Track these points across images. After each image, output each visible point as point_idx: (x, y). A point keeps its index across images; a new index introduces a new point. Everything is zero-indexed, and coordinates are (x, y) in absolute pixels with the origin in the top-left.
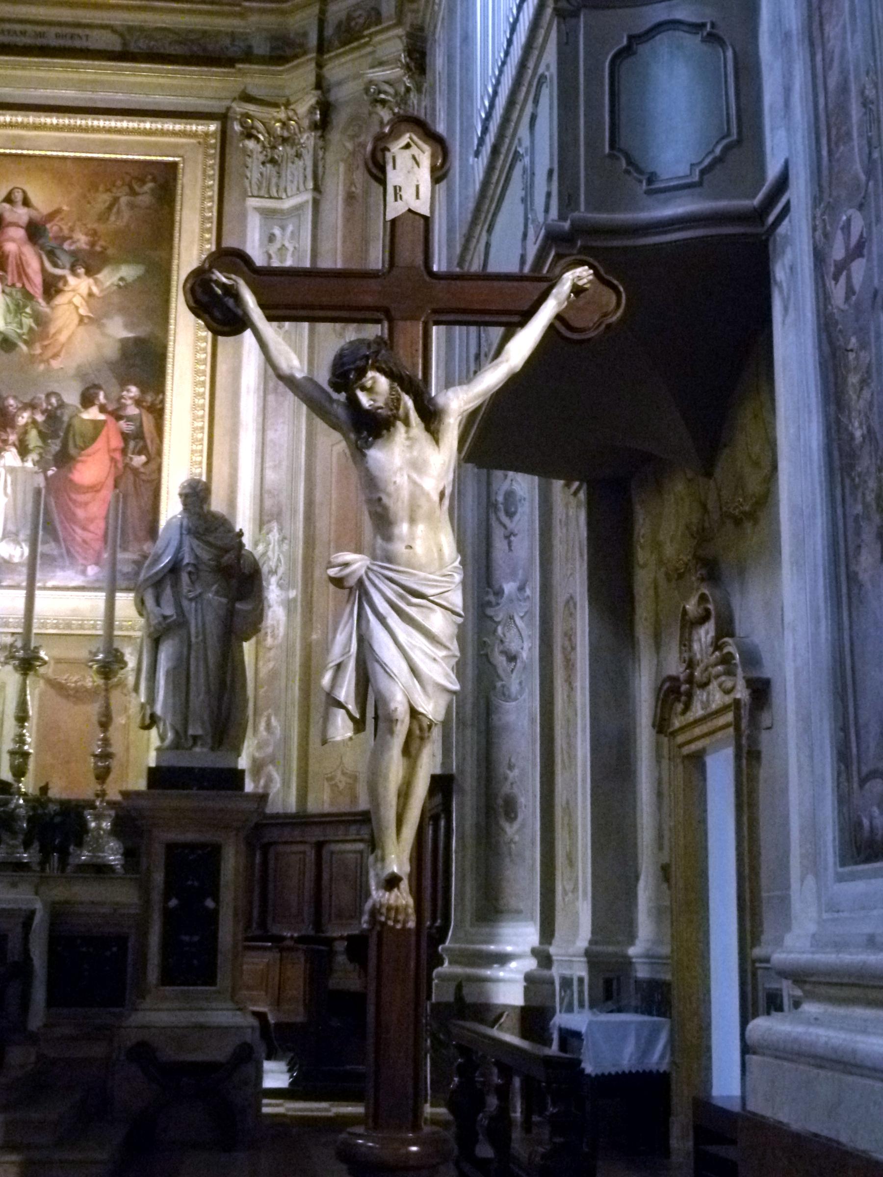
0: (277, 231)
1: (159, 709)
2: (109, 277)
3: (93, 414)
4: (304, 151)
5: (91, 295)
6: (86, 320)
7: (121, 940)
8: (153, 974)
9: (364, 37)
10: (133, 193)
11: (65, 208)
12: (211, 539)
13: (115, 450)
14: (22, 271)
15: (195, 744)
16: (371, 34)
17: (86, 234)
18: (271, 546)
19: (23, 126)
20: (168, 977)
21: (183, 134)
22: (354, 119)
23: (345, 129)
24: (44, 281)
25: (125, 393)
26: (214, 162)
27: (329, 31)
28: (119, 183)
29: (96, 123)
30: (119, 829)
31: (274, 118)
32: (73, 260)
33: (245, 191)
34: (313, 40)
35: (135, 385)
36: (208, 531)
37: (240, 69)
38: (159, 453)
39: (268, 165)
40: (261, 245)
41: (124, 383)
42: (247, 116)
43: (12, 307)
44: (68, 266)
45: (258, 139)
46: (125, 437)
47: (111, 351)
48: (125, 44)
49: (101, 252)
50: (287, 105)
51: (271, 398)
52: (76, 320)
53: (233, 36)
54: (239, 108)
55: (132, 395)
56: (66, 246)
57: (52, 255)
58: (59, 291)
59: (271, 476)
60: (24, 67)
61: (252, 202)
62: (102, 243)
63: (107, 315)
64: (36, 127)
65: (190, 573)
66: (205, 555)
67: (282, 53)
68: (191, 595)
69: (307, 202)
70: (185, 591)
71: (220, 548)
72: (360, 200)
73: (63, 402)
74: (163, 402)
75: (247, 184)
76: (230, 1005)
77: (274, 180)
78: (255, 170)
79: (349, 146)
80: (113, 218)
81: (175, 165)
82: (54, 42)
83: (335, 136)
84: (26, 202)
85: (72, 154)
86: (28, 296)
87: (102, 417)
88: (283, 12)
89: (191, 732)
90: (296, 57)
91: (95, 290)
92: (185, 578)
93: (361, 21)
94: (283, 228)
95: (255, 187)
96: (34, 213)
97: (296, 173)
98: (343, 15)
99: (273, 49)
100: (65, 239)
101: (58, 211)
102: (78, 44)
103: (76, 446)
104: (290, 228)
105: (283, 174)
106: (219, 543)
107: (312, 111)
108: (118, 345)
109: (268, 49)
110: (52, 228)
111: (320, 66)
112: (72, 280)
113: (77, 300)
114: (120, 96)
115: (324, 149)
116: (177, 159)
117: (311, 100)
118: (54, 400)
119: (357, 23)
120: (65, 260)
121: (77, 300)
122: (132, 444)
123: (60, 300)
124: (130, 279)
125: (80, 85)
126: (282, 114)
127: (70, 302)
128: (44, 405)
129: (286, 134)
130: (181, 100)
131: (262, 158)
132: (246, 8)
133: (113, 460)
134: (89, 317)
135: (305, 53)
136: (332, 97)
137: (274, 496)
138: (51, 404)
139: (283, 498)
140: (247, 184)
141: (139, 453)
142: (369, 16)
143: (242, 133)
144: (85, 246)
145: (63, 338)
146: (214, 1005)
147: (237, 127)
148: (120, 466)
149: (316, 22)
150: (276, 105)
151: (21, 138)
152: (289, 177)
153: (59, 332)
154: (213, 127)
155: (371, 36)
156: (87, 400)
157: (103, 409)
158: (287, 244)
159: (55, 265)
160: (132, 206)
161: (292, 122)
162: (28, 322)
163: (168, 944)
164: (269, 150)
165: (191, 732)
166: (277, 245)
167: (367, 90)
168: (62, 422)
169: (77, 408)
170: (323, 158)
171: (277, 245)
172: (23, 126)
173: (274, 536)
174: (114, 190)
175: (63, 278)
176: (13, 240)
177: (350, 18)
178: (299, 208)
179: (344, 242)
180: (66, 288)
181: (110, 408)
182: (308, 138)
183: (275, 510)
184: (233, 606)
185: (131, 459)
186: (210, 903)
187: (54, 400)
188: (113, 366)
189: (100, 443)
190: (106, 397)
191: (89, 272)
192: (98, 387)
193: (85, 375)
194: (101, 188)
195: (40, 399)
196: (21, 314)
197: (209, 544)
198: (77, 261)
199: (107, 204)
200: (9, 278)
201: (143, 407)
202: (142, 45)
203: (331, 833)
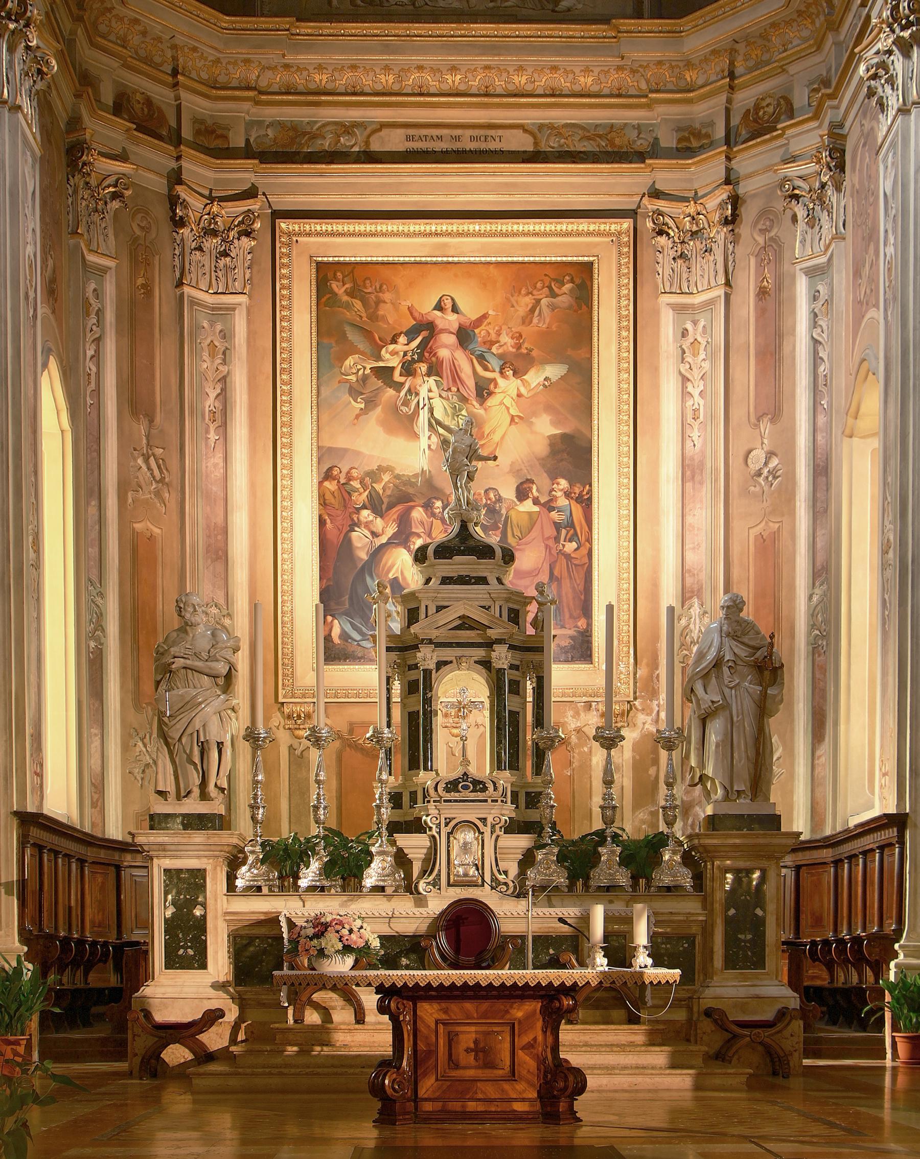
0: (689, 326)
1: (709, 771)
2: (535, 378)
3: (528, 506)
4: (714, 246)
5: (519, 395)
6: (517, 420)
7: (691, 939)
8: (718, 961)
9: (777, 130)
10: (553, 295)
11: (491, 312)
12: (746, 640)
13: (549, 538)
14: (456, 377)
15: (739, 796)
16: (784, 127)
17: (512, 338)
18: (692, 620)
19: (449, 234)
20: (731, 962)
21: (599, 234)
22: (765, 213)
23: (756, 223)
24: (476, 384)
25: (555, 486)
26: (626, 260)
27: (735, 121)
28: (539, 285)
29: (515, 227)
30: (687, 859)
31: (683, 212)
32: (501, 363)
33: (657, 287)
34: (720, 132)
35: (564, 477)
36: (744, 634)
37: (650, 165)
38: (589, 540)
39: (680, 261)
40: (675, 341)
41: (553, 478)
42: (661, 214)
43: (449, 411)
44: (498, 369)
45: (668, 234)
46: (557, 526)
47: (542, 448)
48: (536, 144)
49: (528, 354)
50: (696, 198)
51: (689, 485)
52: (509, 419)
53: (639, 128)
54: (650, 205)
55: (561, 487)
56: (494, 350)
57: (481, 358)
58: (490, 394)
59: (689, 556)
60: (443, 174)
61: (665, 299)
62: (526, 345)
63: (535, 414)
64: (460, 234)
65: (730, 667)
66: (742, 652)
67: (688, 145)
68: (732, 684)
69: (720, 296)
70: (726, 682)
71: (753, 648)
72: (773, 295)
73: (500, 496)
74: (590, 492)
75: (660, 281)
76: (777, 983)
77: (685, 276)
78: (666, 265)
79: (760, 240)
80: (535, 320)
81: (591, 264)
82: (472, 146)
83: (744, 230)
84: (455, 309)
85: (494, 259)
86: (464, 399)
87: (536, 509)
88: (689, 101)
89: (736, 788)
90: (702, 148)
91: (523, 391)
92: (725, 669)
93: (770, 110)
94: (695, 323)
95: (667, 284)
96: (463, 320)
97: (706, 267)
98: (750, 104)
99: (680, 140)
100: (492, 343)
101: (485, 316)
102: (493, 146)
103: (513, 535)
104: (702, 323)
105: (693, 269)
106: (752, 643)
107: (722, 206)
108: (547, 442)
109: (675, 142)
110: (480, 333)
111: (729, 159)
112: (500, 381)
113: (508, 401)
114: (535, 198)
115: (735, 242)
116: (591, 259)
118: (492, 495)
119: (765, 112)
120: (495, 363)
121: (508, 401)
122: (564, 532)
123: (492, 402)
124: (554, 379)
126: (692, 209)
127: (502, 403)
128: (484, 501)
129: (695, 228)
130: (592, 198)
131: (672, 253)
132: (651, 99)
133: (547, 547)
134: (518, 416)
135: (712, 145)
136: (741, 191)
137: (694, 575)
138: (490, 499)
139: (704, 577)
140: (660, 281)
141: (570, 541)
142: (779, 104)
143: (654, 230)
144: (511, 349)
145: (496, 437)
146: (765, 982)
147: (649, 225)
148: (554, 552)
149: (723, 112)
150: (685, 200)
151: (445, 245)
152: (699, 272)
153: (493, 431)
154: (626, 224)
155: (784, 129)
156: (522, 494)
157: (536, 502)
158: (699, 339)
159: (486, 369)
160: (553, 307)
161: (701, 216)
163: (730, 941)
164: (679, 245)
165: (736, 788)
166: (690, 339)
167: (782, 186)
168: (502, 515)
169: (513, 501)
170: (733, 252)
171: (690, 339)
172: (449, 234)
173: (696, 610)
174: (535, 292)
175: (494, 380)
176: (446, 346)
177: (757, 107)
178: (711, 302)
179: (756, 336)
180: (497, 390)
181: (543, 500)
182: (718, 232)
183: (696, 587)
184: (766, 692)
185: (564, 546)
186: (759, 912)
187: (492, 495)
188: (542, 461)
189: (535, 533)
190: (538, 490)
191: (516, 373)
192: (532, 482)
193: (518, 471)
194: (523, 291)
195: (480, 494)
196: (458, 416)
197: (743, 643)
198: (505, 363)
199: (530, 306)
200: (445, 382)
201: (572, 498)
202: (552, 144)
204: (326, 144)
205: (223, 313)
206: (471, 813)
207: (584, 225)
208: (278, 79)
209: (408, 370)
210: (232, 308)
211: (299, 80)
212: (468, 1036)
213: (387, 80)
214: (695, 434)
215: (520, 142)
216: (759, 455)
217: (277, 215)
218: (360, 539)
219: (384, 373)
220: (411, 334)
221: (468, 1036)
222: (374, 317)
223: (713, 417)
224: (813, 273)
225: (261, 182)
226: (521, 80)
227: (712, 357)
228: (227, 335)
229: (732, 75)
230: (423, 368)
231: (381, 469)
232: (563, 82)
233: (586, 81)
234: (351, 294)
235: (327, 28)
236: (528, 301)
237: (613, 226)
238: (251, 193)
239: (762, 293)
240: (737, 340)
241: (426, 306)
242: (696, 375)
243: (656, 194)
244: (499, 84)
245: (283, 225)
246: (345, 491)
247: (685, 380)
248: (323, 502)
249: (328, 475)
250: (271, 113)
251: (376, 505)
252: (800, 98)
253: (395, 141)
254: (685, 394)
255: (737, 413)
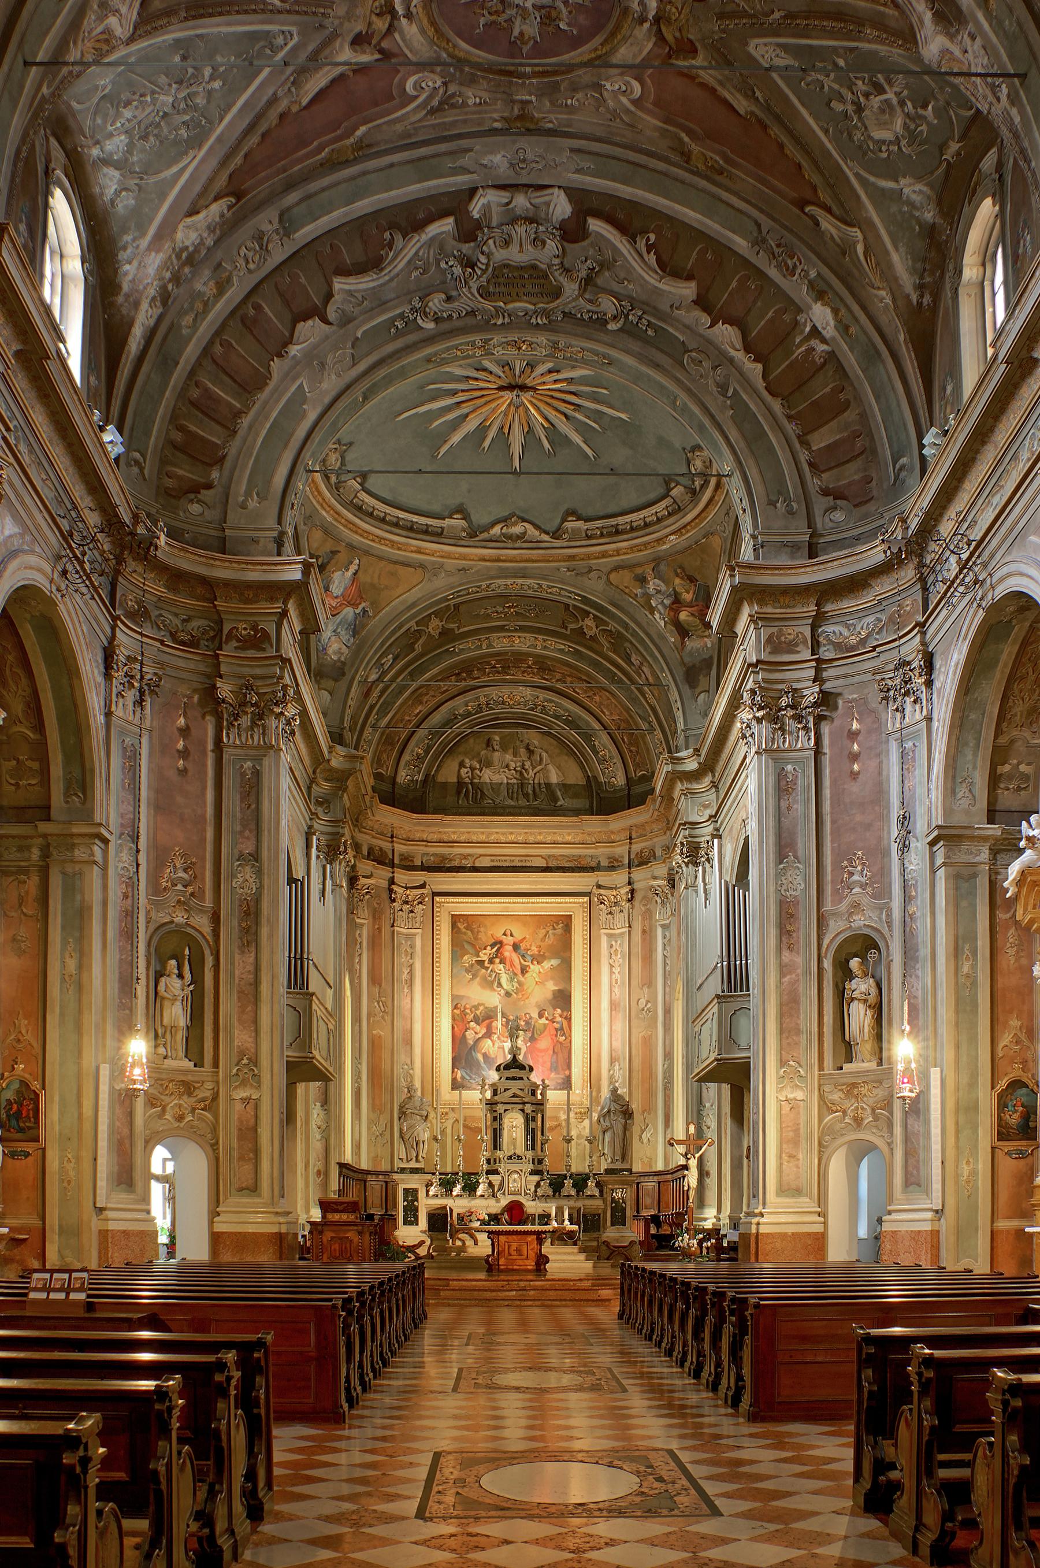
2: (547, 965)
3: (543, 1021)
14: (512, 964)
22: (644, 898)
34: (626, 861)
47: (550, 996)
54: (596, 891)
57: (523, 956)
78: (603, 917)
83: (636, 903)
110: (523, 946)
117: (627, 889)
120: (529, 959)
125: (530, 883)
154: (586, 899)
156: (541, 1016)
162: (516, 985)
178: (622, 934)
188: (550, 1001)
203: (642, 1179)
204: (456, 863)
205: (411, 937)
206: (517, 1168)
207: (568, 899)
208: (435, 837)
209: (491, 961)
210: (415, 935)
211: (445, 838)
212: (514, 1246)
213: (483, 838)
214: (616, 990)
215: (541, 863)
216: (643, 1001)
217: (435, 894)
218: (470, 1034)
219: (481, 963)
220: (493, 946)
221: (514, 1246)
222: (476, 939)
223: (623, 983)
224: (664, 927)
225: (428, 881)
226: (540, 838)
227: (623, 957)
228: (412, 946)
229: (631, 838)
230: (497, 960)
231: (479, 1004)
232: (560, 839)
233: (569, 838)
234: (466, 928)
235: (457, 818)
236: (543, 932)
237: (581, 900)
238: (423, 886)
239: (644, 932)
240: (634, 951)
241: (499, 934)
242: (616, 964)
243: (599, 886)
244: (531, 839)
245: (437, 899)
246: (464, 1014)
247: (612, 966)
248: (453, 1019)
249: (456, 1007)
250: (432, 850)
251: (477, 1020)
252: (658, 852)
253: (486, 862)
254: (612, 973)
255: (634, 982)
